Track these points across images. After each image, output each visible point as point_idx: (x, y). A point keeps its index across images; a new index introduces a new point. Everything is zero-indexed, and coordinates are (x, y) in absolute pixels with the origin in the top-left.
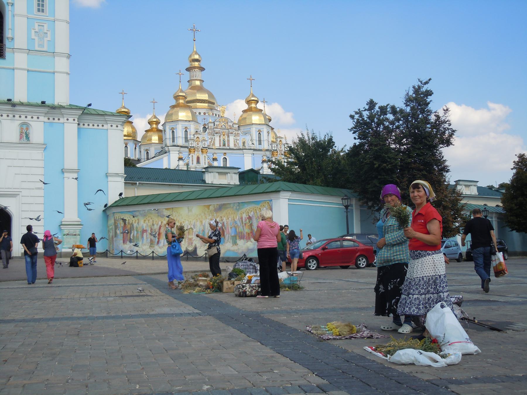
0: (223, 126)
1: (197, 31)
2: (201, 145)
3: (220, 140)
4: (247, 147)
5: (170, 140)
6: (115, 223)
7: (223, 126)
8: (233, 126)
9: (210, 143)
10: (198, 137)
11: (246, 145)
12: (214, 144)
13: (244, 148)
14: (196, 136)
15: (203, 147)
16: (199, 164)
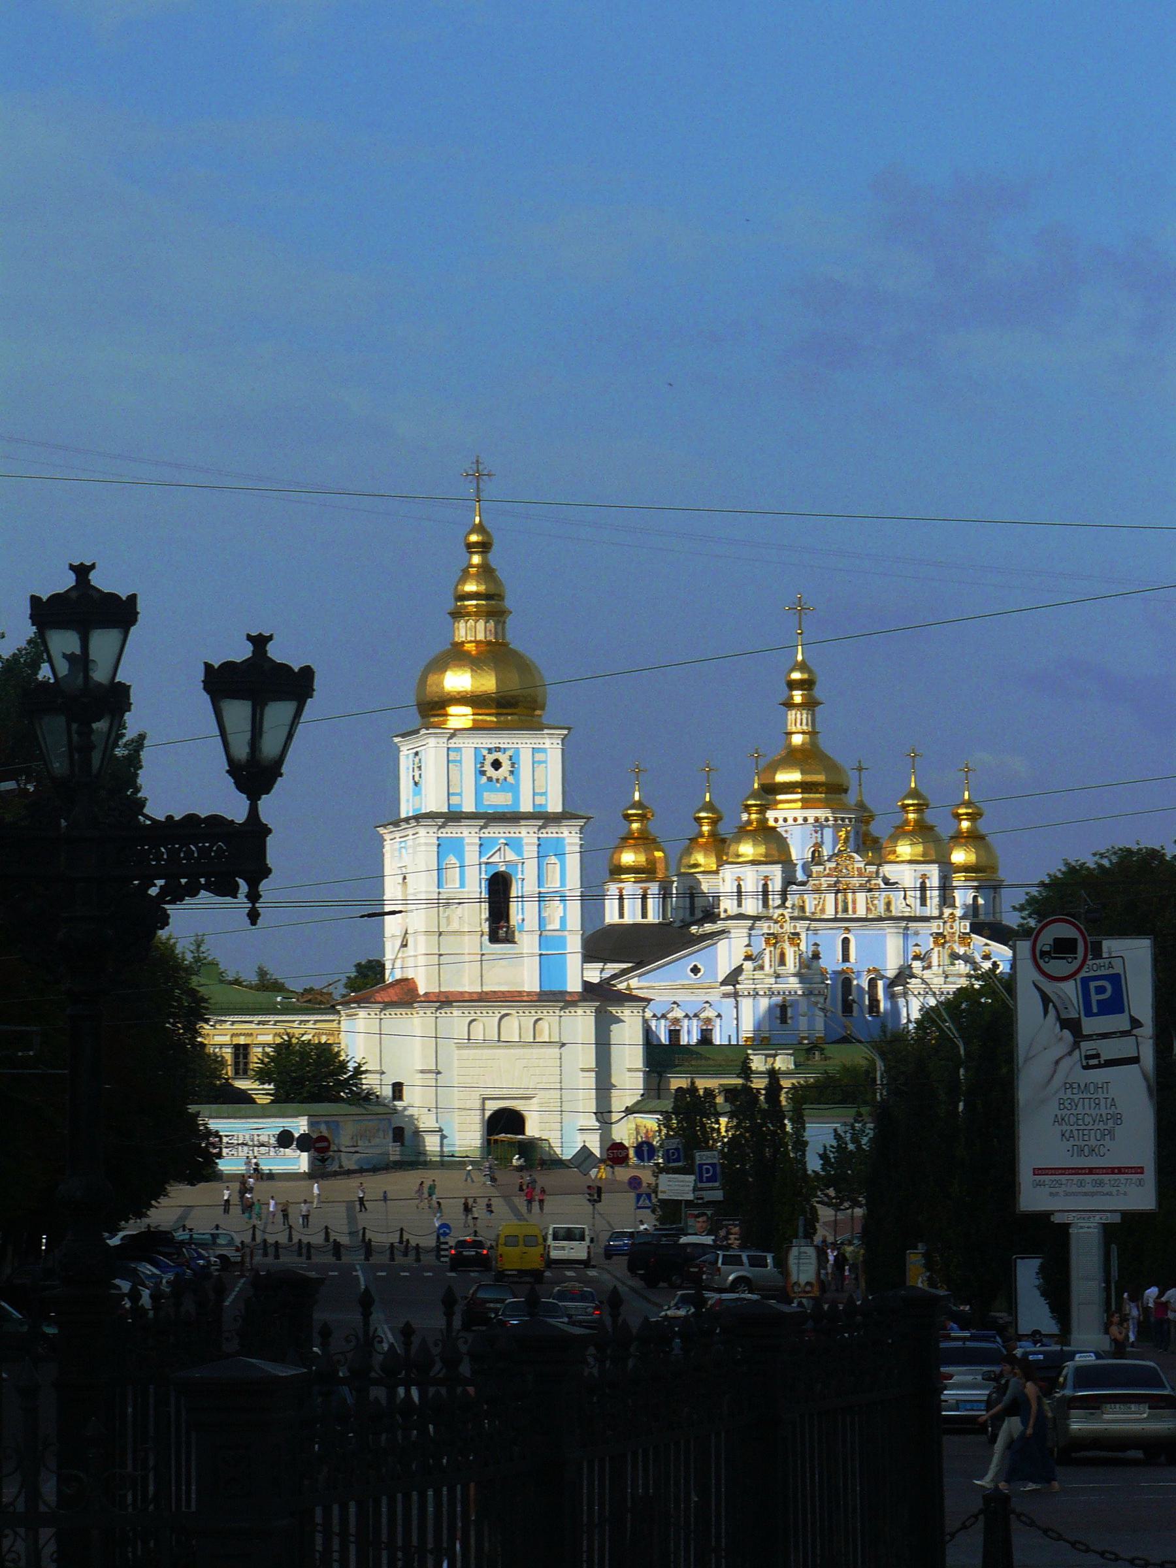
0: (844, 871)
1: (806, 609)
2: (789, 927)
3: (836, 899)
4: (894, 914)
5: (732, 904)
6: (636, 1128)
7: (844, 871)
8: (865, 869)
9: (815, 909)
10: (782, 915)
11: (893, 908)
12: (823, 911)
13: (889, 914)
14: (780, 911)
15: (793, 934)
16: (783, 968)
